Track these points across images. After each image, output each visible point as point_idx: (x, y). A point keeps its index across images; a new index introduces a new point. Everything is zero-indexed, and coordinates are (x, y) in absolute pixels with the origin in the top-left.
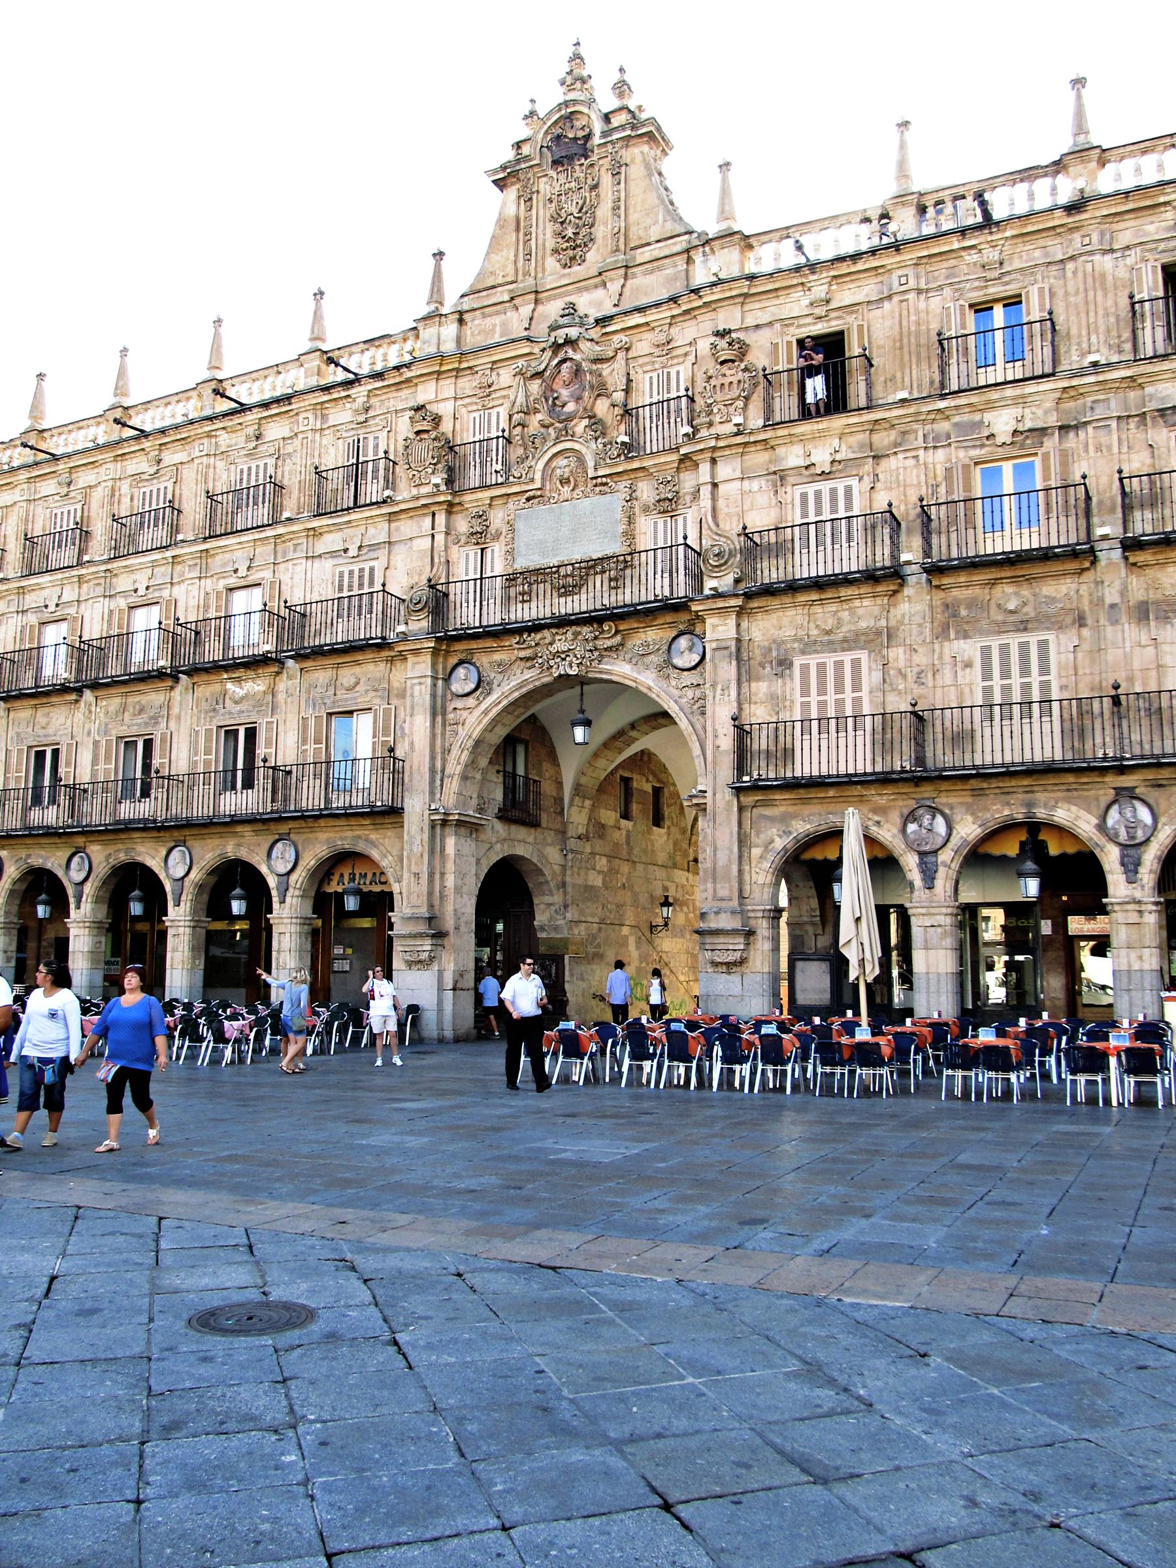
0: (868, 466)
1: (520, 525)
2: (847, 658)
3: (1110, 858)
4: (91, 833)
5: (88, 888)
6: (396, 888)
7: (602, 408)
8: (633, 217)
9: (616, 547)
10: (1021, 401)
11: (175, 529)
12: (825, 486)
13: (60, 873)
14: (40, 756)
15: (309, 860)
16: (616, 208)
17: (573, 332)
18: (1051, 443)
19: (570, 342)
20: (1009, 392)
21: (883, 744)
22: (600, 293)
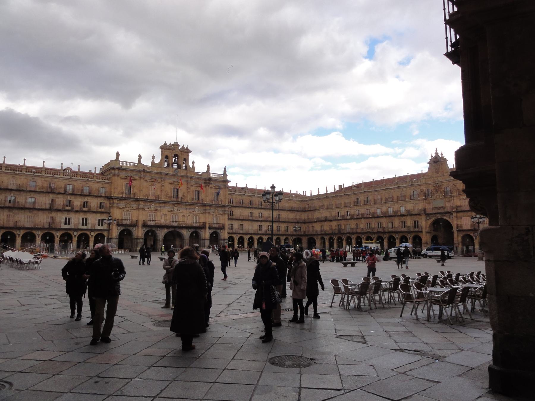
2: (468, 218)
4: (386, 233)
5: (386, 238)
7: (441, 190)
9: (444, 206)
11: (393, 199)
14: (378, 224)
15: (412, 236)
17: (438, 182)
19: (437, 183)
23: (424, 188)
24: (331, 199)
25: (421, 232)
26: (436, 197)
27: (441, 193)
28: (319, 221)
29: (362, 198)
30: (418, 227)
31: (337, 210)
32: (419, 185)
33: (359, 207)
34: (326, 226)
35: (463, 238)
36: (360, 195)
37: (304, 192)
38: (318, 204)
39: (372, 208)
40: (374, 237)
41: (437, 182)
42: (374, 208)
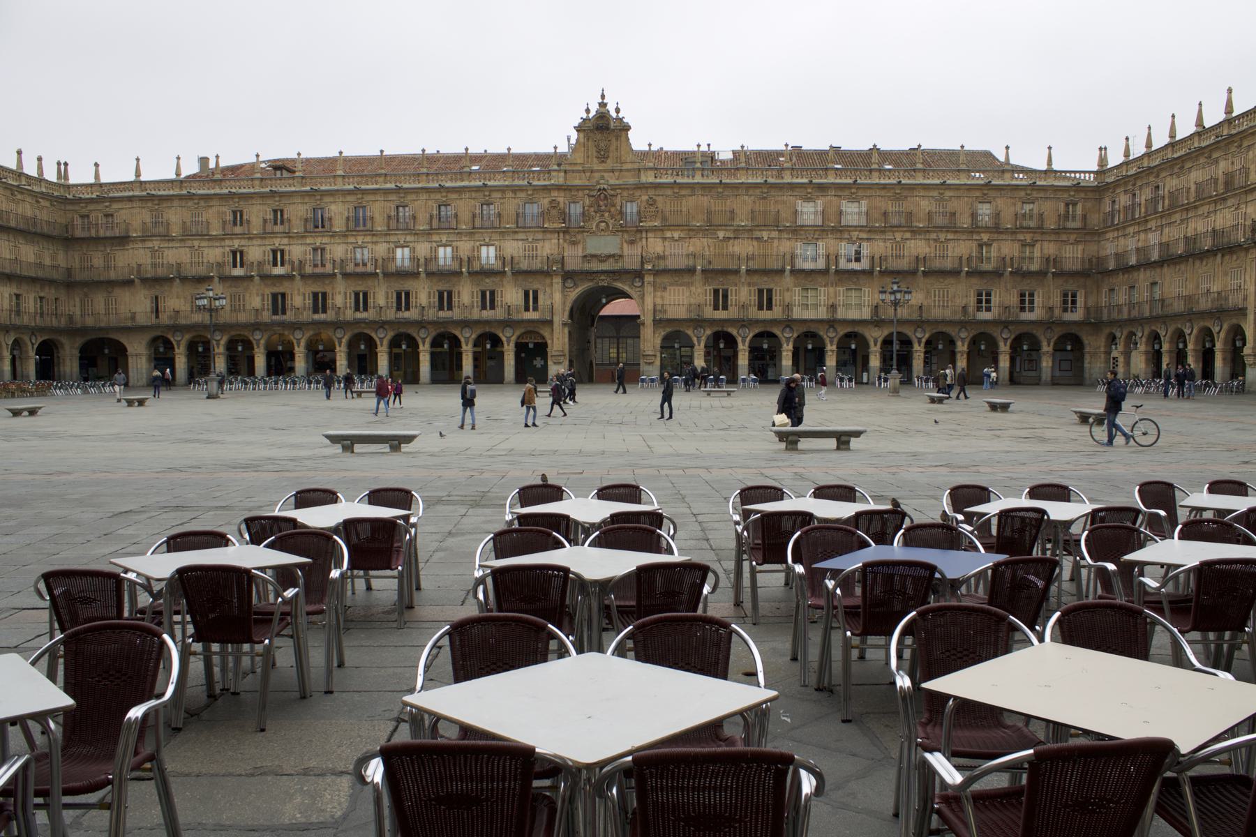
0: (687, 240)
1: (588, 240)
2: (681, 288)
3: (739, 340)
6: (549, 342)
8: (622, 153)
9: (617, 251)
10: (726, 230)
12: (676, 243)
13: (415, 335)
15: (518, 333)
16: (617, 149)
17: (606, 187)
18: (731, 241)
19: (604, 189)
20: (723, 228)
21: (689, 311)
22: (611, 174)
23: (561, 198)
24: (202, 203)
25: (550, 323)
26: (597, 225)
27: (612, 217)
28: (144, 281)
29: (338, 211)
30: (535, 309)
31: (227, 242)
32: (546, 189)
33: (326, 240)
34: (178, 297)
35: (666, 338)
36: (327, 199)
37: (62, 167)
38: (135, 218)
39: (376, 243)
40: (382, 336)
41: (602, 186)
42: (385, 246)
